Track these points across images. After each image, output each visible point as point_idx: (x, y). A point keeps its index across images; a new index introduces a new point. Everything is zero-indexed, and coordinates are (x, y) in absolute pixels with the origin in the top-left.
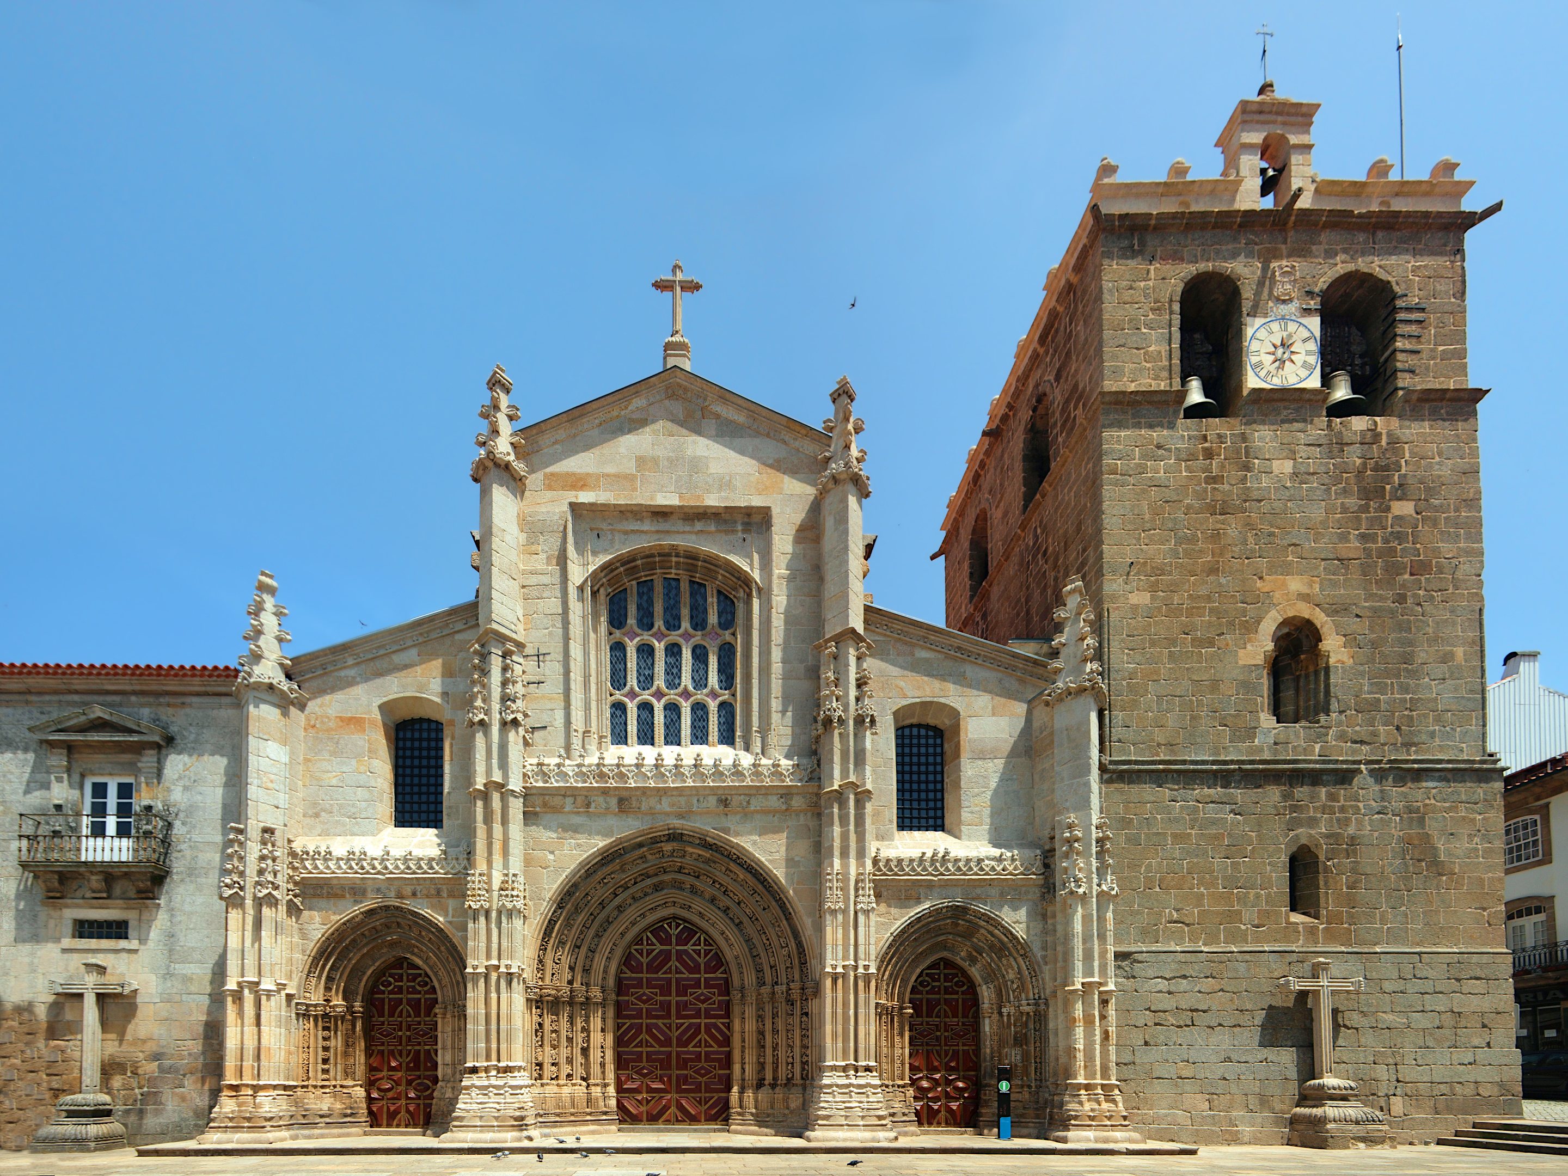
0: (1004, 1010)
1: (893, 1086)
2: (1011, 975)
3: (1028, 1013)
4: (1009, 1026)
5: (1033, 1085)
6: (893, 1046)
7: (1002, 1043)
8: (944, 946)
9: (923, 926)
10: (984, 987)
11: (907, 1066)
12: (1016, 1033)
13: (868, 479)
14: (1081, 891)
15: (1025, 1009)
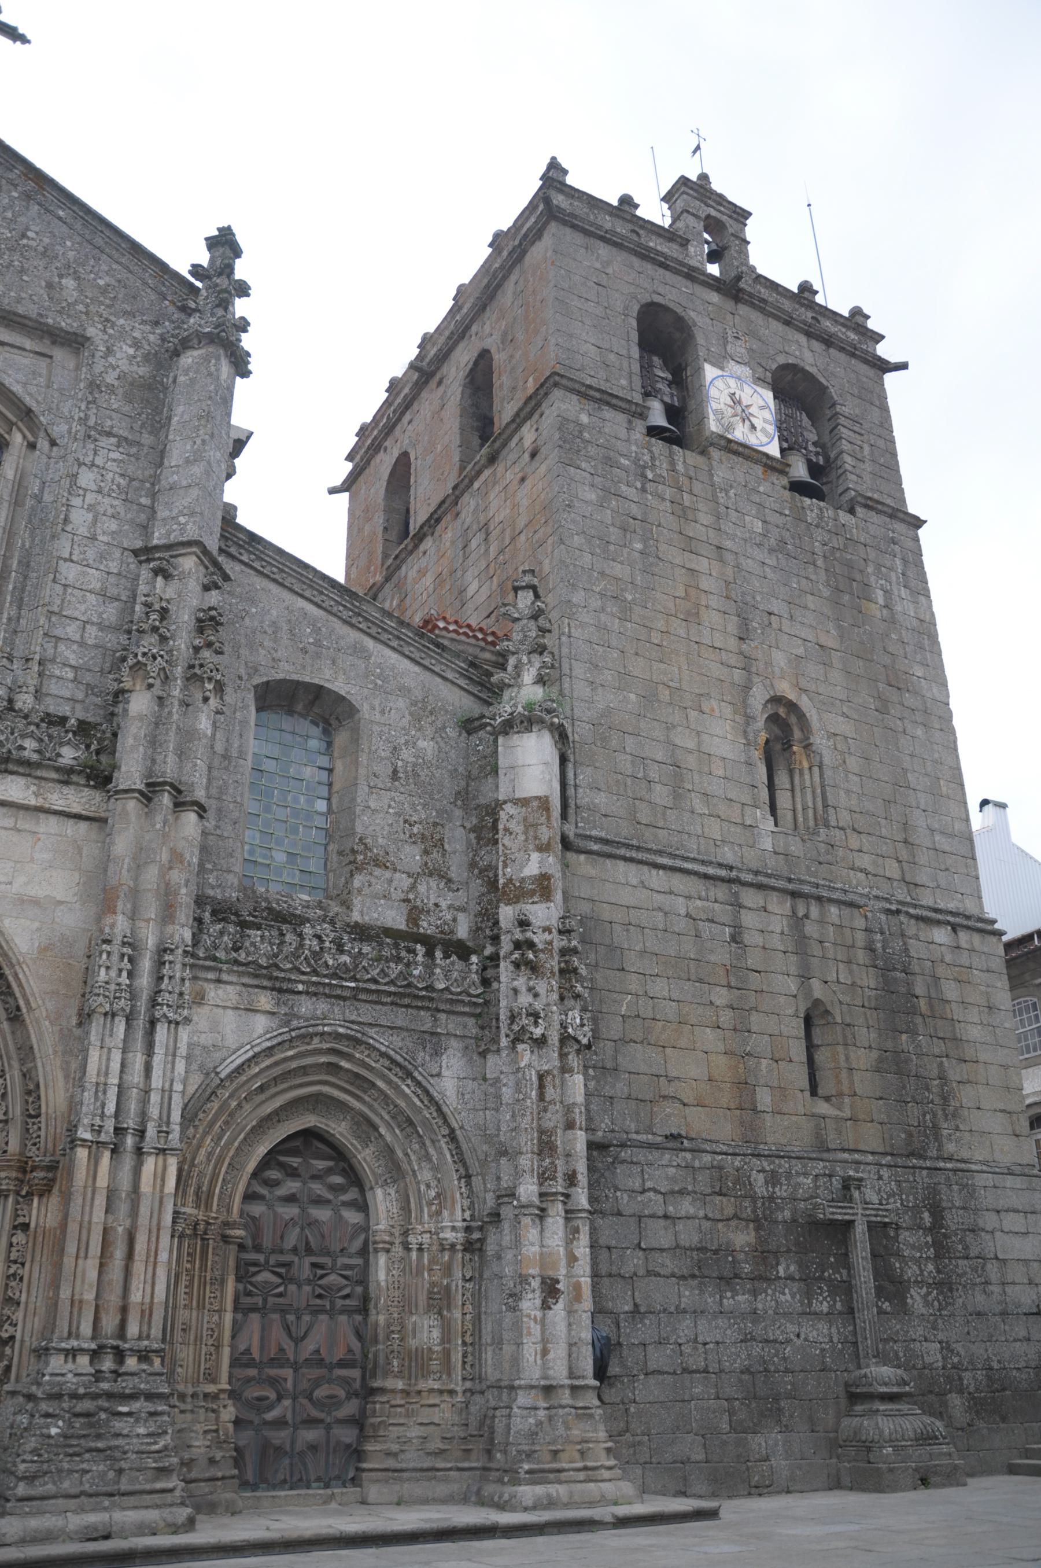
0: (411, 1239)
1: (194, 1396)
2: (425, 1175)
3: (453, 1246)
4: (419, 1273)
5: (459, 1389)
6: (201, 1306)
7: (407, 1305)
8: (316, 1102)
9: (276, 1064)
10: (379, 1192)
11: (226, 1351)
12: (433, 1284)
13: (248, 355)
14: (538, 1032)
15: (449, 1235)
